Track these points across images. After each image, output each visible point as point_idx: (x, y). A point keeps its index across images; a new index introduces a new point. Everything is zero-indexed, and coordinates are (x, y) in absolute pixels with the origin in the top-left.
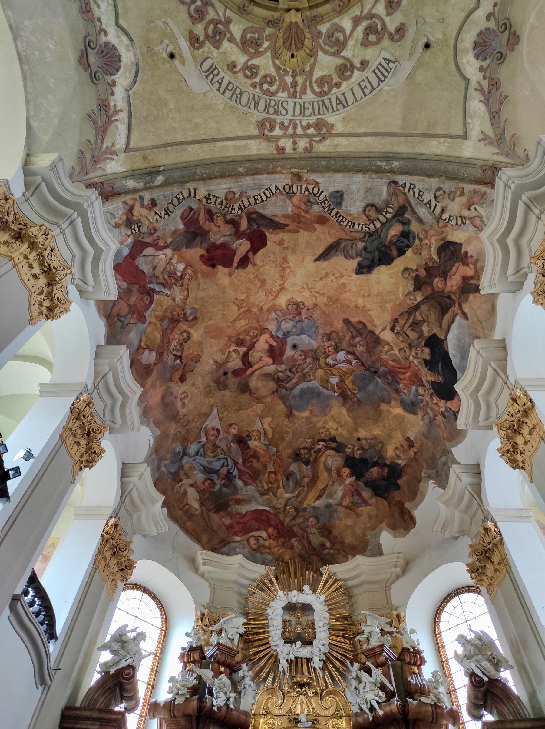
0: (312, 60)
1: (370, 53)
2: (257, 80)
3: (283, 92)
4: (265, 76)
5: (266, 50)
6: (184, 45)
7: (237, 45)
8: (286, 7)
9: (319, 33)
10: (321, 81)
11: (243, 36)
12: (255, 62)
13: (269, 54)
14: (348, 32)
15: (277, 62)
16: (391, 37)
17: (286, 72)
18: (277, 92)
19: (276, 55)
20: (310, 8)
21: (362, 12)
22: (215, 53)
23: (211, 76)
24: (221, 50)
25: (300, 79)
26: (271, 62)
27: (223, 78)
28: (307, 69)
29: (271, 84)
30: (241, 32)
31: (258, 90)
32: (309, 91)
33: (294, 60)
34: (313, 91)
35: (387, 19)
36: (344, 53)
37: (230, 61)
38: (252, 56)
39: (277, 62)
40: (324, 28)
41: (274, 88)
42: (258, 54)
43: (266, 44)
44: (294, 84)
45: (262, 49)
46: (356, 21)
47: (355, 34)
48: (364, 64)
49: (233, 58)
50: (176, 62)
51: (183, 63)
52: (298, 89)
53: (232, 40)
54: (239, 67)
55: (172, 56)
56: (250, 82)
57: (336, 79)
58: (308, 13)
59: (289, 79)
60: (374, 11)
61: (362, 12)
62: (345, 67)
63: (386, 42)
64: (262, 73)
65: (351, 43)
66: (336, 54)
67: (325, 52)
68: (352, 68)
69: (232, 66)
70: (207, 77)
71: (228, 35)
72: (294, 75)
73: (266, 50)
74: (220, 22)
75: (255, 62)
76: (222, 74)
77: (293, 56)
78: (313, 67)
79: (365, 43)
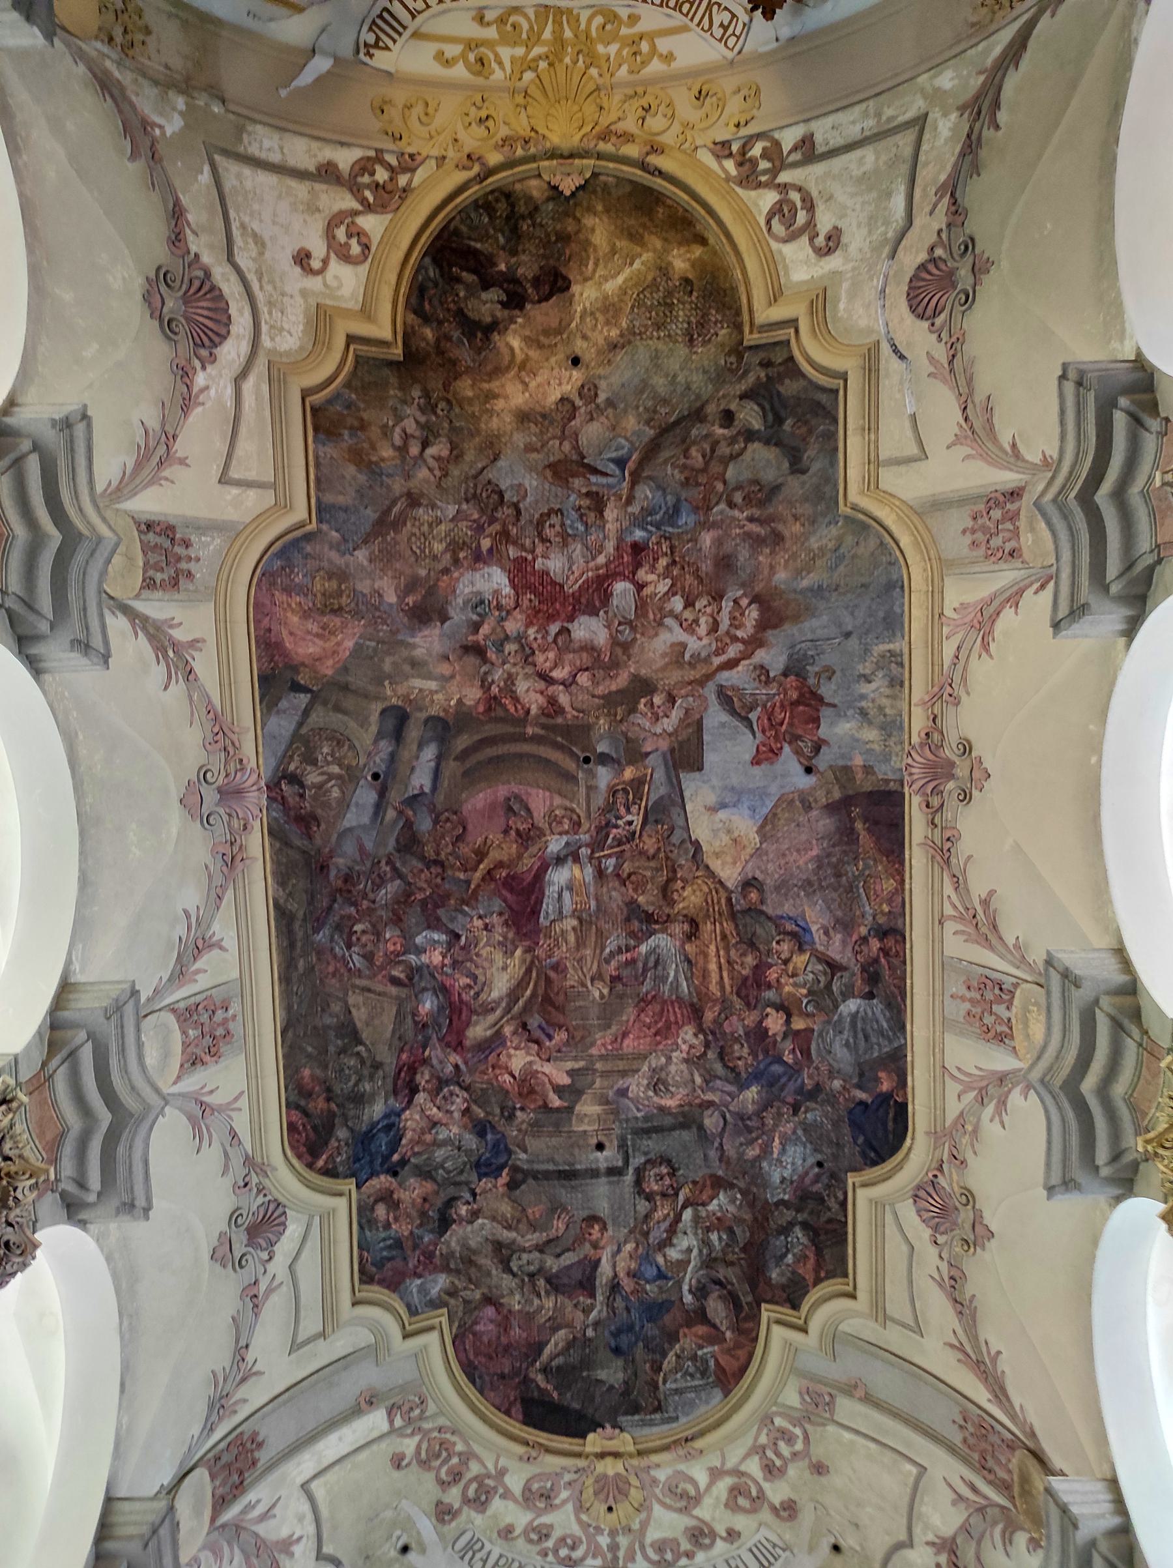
0: (643, 1515)
1: (741, 1522)
2: (550, 1544)
3: (594, 1557)
4: (563, 1540)
5: (564, 1502)
6: (426, 1527)
7: (515, 1501)
8: (598, 1450)
9: (655, 1481)
10: (660, 1546)
11: (527, 1489)
12: (546, 1519)
13: (570, 1507)
14: (702, 1485)
15: (584, 1517)
16: (774, 1510)
17: (599, 1530)
18: (583, 1559)
19: (580, 1508)
20: (640, 1453)
21: (723, 1464)
22: (478, 1519)
23: (470, 1553)
24: (489, 1512)
25: (623, 1541)
26: (573, 1518)
27: (489, 1553)
28: (636, 1526)
29: (573, 1548)
30: (522, 1483)
31: (550, 1558)
32: (639, 1557)
33: (613, 1516)
34: (646, 1557)
35: (766, 1486)
36: (697, 1512)
37: (502, 1525)
38: (540, 1513)
39: (584, 1517)
40: (662, 1475)
41: (577, 1554)
42: (551, 1507)
43: (564, 1494)
44: (614, 1547)
45: (557, 1501)
46: (715, 1474)
47: (715, 1490)
48: (732, 1535)
49: (508, 1520)
50: (412, 1556)
51: (423, 1550)
52: (621, 1554)
53: (507, 1495)
54: (518, 1531)
55: (405, 1549)
56: (537, 1548)
57: (685, 1546)
58: (635, 1462)
59: (604, 1541)
60: (743, 1468)
61: (723, 1464)
62: (702, 1532)
63: (766, 1515)
64: (557, 1534)
65: (707, 1501)
66: (685, 1510)
67: (663, 1504)
68: (713, 1535)
69: (507, 1533)
70: (462, 1558)
71: (501, 1491)
72: (613, 1533)
73: (564, 1502)
74: (489, 1476)
75: (546, 1519)
76: (488, 1547)
77: (610, 1509)
78: (644, 1525)
79: (732, 1504)
